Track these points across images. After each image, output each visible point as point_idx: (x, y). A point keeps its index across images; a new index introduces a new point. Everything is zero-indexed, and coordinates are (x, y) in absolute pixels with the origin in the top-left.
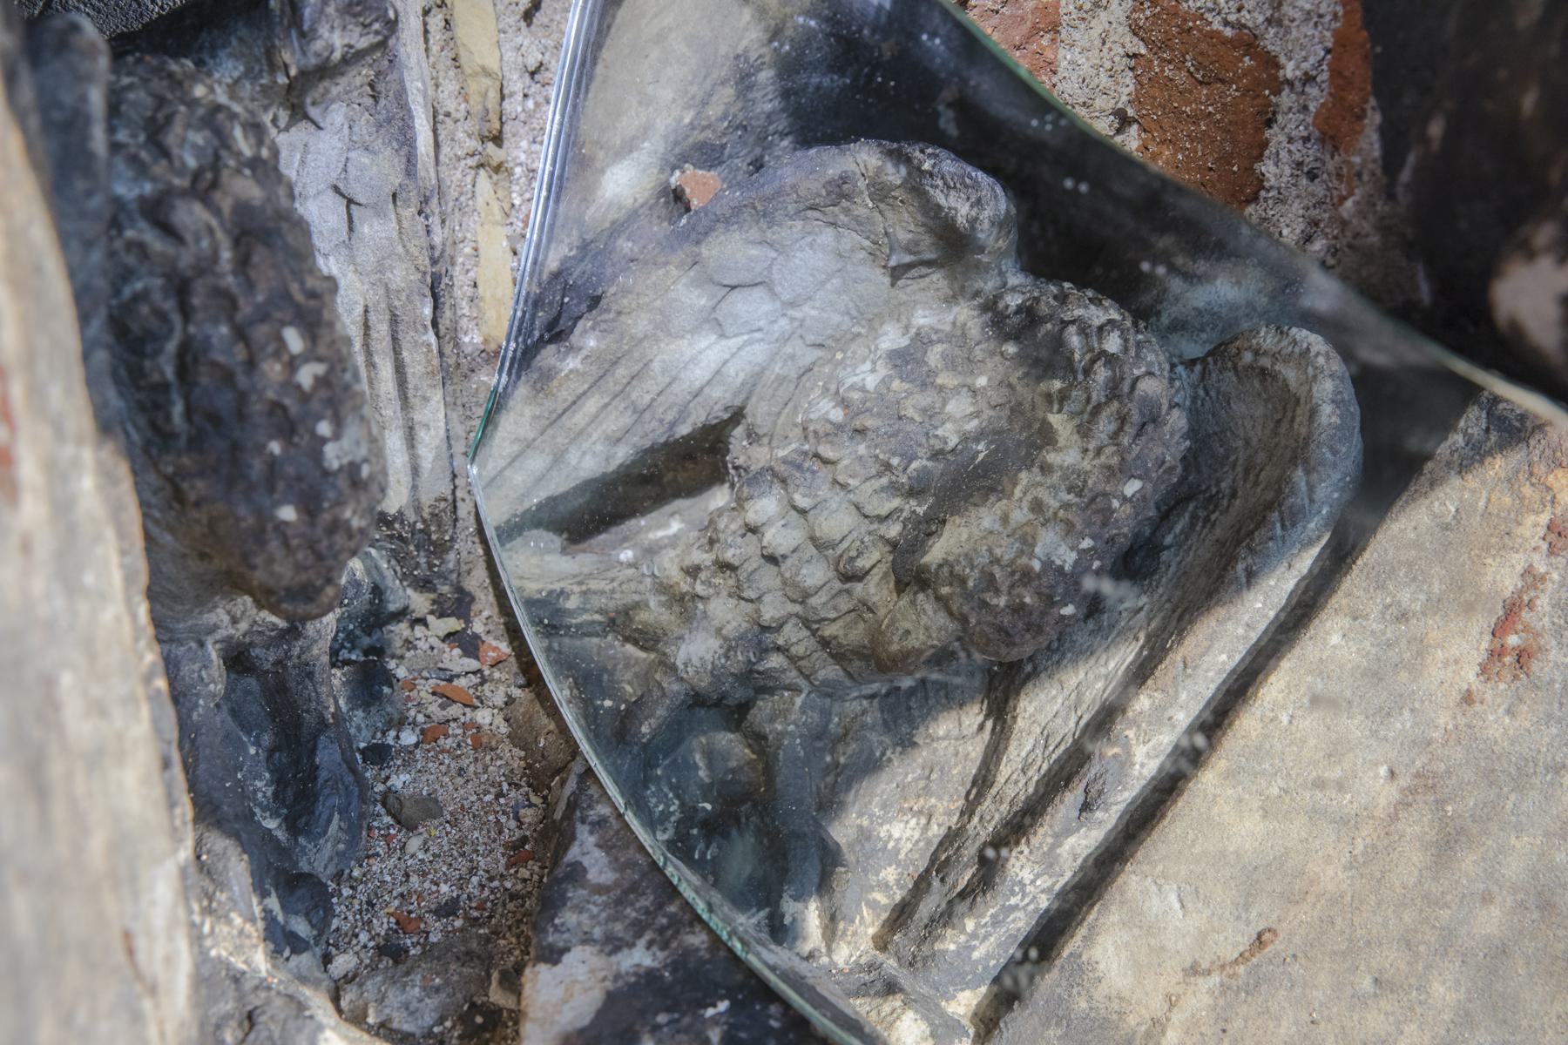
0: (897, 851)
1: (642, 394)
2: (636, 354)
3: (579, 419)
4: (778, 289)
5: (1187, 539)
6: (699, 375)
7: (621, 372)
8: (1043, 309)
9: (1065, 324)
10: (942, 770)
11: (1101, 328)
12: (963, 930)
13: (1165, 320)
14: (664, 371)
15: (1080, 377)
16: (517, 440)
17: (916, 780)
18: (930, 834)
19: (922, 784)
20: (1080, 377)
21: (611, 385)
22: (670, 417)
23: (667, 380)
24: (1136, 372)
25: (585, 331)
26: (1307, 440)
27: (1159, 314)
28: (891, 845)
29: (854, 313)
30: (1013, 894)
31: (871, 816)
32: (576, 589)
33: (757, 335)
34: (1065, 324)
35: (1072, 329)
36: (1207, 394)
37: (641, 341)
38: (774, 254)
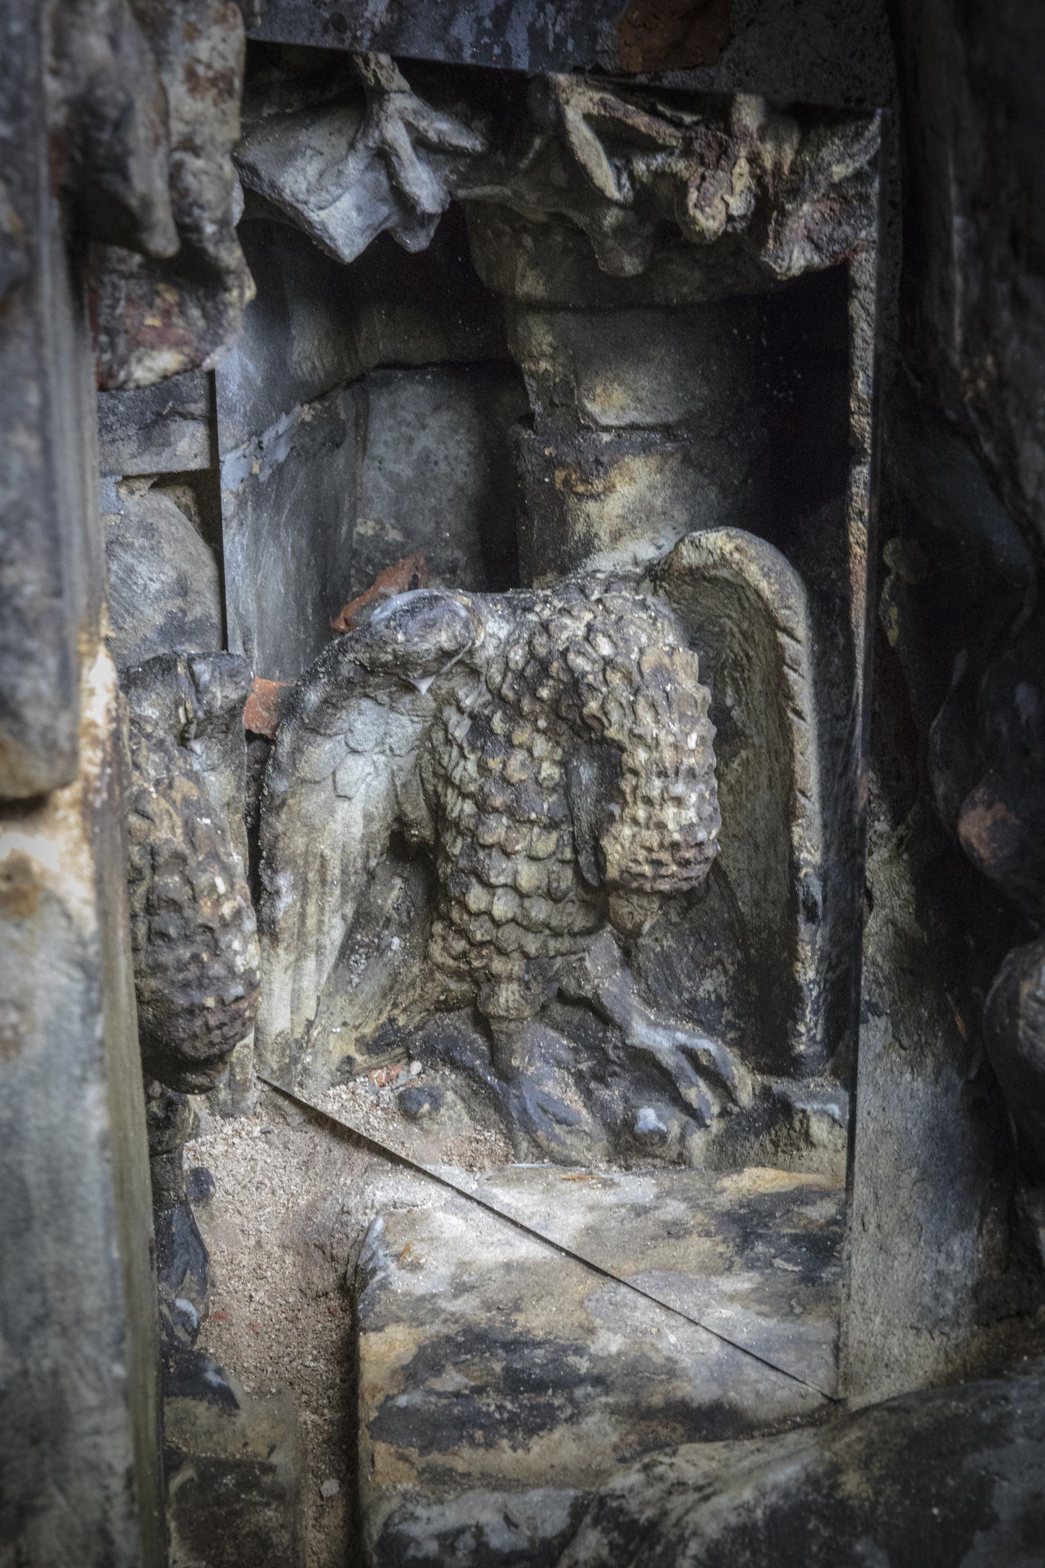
0: (719, 997)
1: (334, 871)
2: (311, 859)
3: (311, 922)
4: (360, 749)
5: (740, 697)
6: (358, 830)
7: (312, 876)
8: (542, 651)
9: (564, 654)
10: (705, 928)
11: (587, 639)
12: (801, 1035)
13: (605, 538)
14: (333, 850)
15: (604, 690)
16: (287, 969)
17: (695, 947)
18: (731, 973)
19: (700, 946)
20: (604, 690)
21: (315, 888)
22: (359, 864)
24: (633, 657)
25: (271, 880)
26: (767, 609)
27: (596, 535)
28: (713, 997)
29: (416, 719)
30: (811, 990)
31: (687, 989)
32: (396, 1012)
33: (368, 779)
34: (564, 654)
35: (571, 656)
36: (678, 603)
37: (307, 851)
38: (340, 737)
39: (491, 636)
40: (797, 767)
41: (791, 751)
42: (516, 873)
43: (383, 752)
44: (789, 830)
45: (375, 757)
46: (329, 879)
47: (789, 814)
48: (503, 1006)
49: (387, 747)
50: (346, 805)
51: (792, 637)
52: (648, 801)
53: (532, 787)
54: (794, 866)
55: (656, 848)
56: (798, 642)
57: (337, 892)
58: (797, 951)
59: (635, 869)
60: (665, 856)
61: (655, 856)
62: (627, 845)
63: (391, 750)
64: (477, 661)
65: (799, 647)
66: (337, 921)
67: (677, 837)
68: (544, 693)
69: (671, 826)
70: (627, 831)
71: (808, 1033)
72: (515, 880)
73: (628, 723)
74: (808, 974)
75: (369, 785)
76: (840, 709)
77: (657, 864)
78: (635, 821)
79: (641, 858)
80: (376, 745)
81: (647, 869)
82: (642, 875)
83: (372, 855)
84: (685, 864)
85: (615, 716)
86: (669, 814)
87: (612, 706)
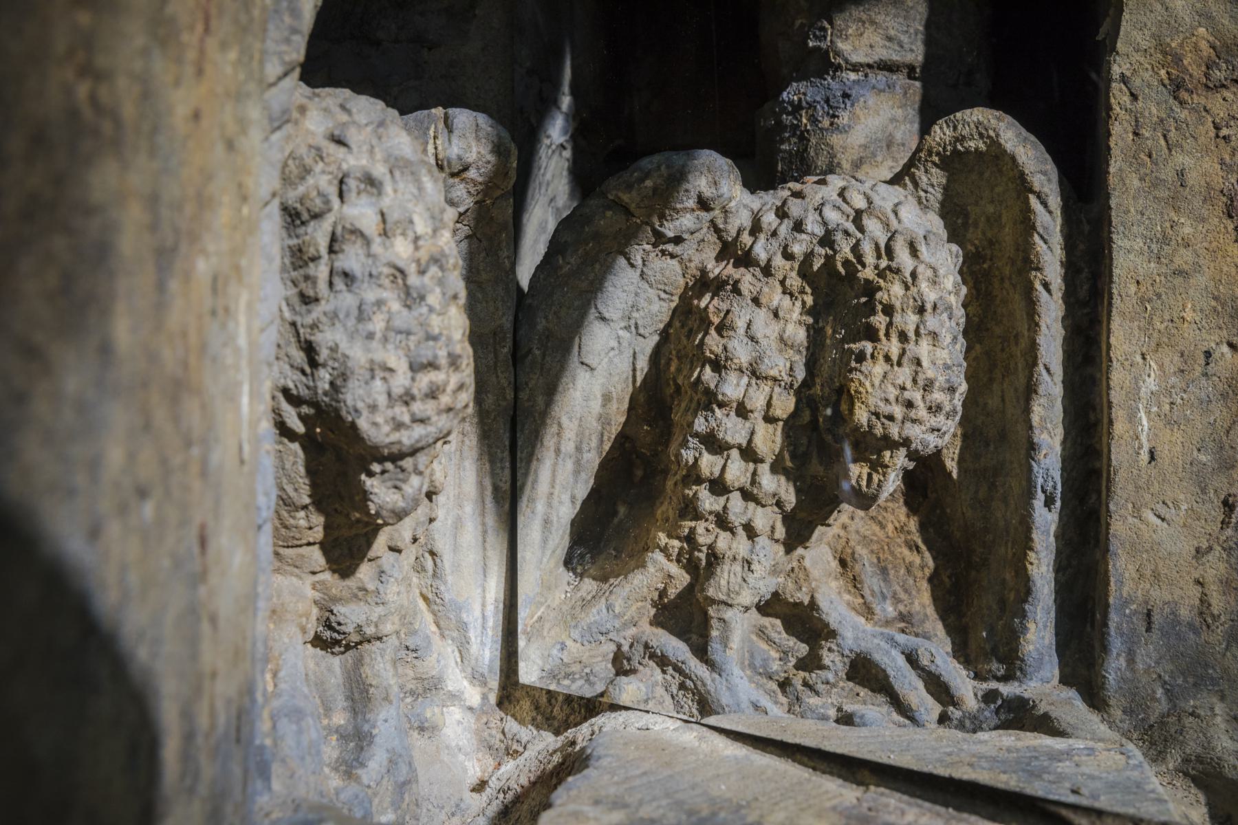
4: (607, 315)
23: (576, 423)
26: (1022, 174)
29: (663, 295)
33: (612, 354)
36: (926, 192)
39: (745, 206)
40: (1041, 340)
41: (1037, 325)
42: (752, 433)
43: (627, 328)
44: (1027, 410)
45: (621, 333)
46: (563, 449)
47: (1030, 390)
48: (725, 590)
49: (632, 322)
50: (588, 375)
51: (1045, 204)
52: (903, 337)
53: (774, 345)
54: (1032, 447)
55: (909, 385)
56: (1050, 212)
57: (570, 465)
58: (1031, 540)
59: (885, 409)
60: (916, 396)
61: (907, 395)
62: (877, 383)
63: (637, 328)
64: (729, 227)
65: (1049, 220)
66: (566, 498)
67: (930, 374)
68: (798, 249)
69: (925, 363)
70: (879, 368)
71: (1039, 634)
72: (750, 441)
73: (884, 263)
74: (1042, 568)
75: (611, 361)
76: (1083, 293)
77: (910, 405)
78: (887, 358)
79: (892, 398)
80: (622, 318)
81: (898, 411)
82: (891, 418)
83: (605, 438)
84: (935, 409)
85: (870, 259)
86: (923, 349)
87: (867, 249)
